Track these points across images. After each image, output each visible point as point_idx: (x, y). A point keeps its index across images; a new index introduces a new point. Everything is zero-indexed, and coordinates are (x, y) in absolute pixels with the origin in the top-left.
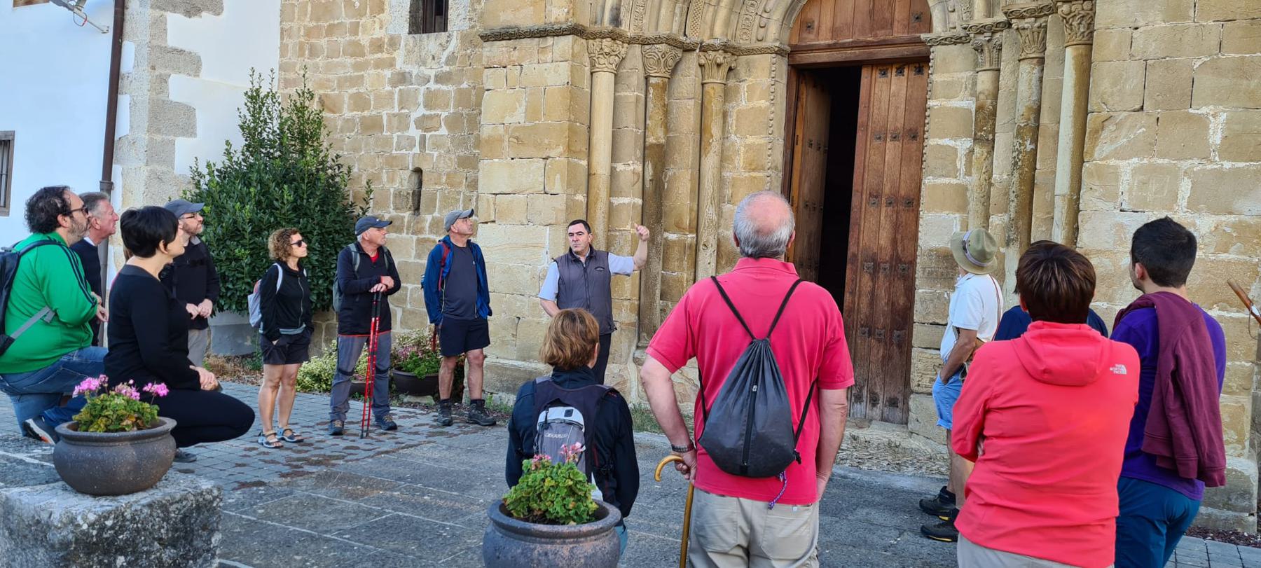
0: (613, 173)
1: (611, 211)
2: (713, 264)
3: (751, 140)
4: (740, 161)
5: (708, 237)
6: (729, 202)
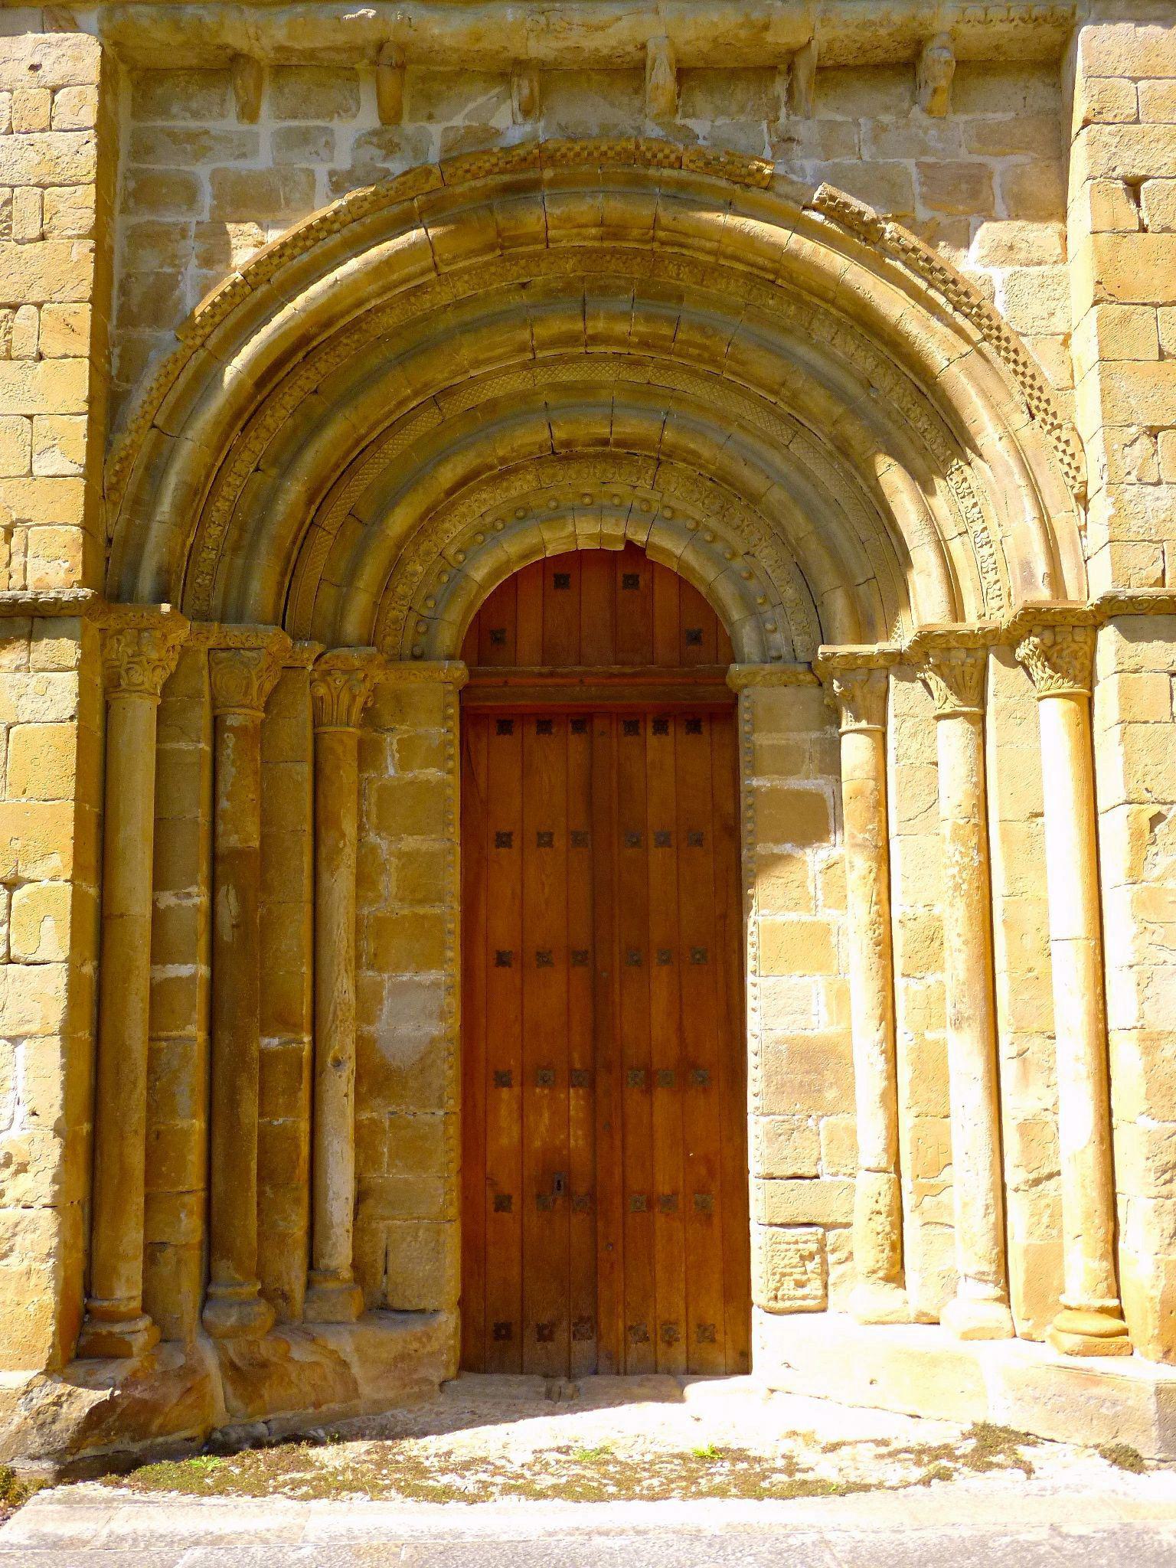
0: (158, 918)
1: (158, 992)
2: (352, 1096)
3: (411, 843)
4: (388, 884)
5: (342, 1044)
6: (371, 967)
